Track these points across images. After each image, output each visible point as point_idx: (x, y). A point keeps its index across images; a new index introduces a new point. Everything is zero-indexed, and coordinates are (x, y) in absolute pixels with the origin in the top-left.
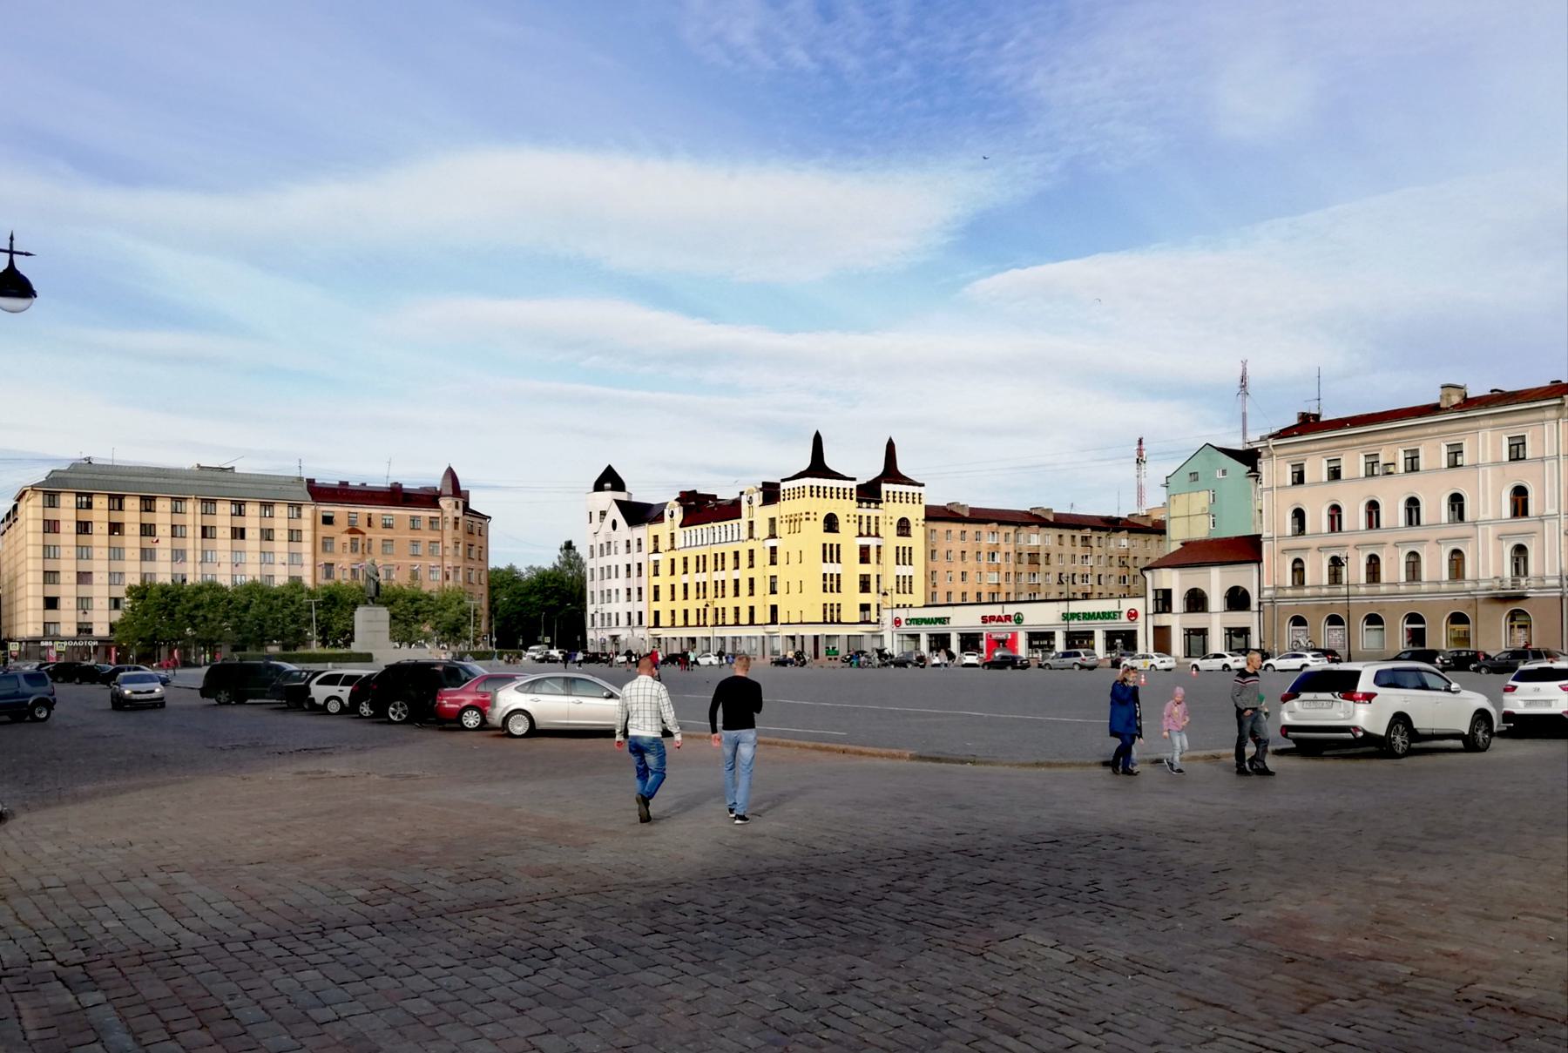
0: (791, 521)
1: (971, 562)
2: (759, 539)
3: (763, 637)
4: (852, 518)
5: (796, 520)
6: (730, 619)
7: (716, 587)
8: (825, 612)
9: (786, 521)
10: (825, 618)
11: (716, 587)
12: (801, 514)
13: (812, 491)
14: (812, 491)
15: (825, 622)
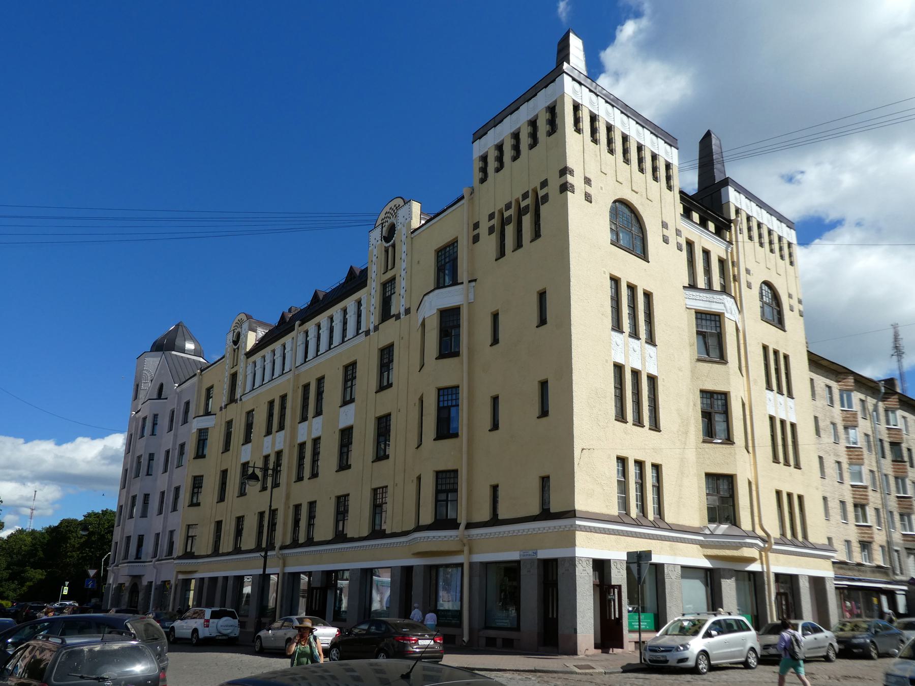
0: (504, 222)
1: (827, 438)
2: (408, 311)
3: (407, 571)
4: (671, 233)
5: (521, 212)
6: (324, 528)
7: (301, 457)
8: (623, 486)
9: (491, 230)
10: (624, 503)
11: (301, 457)
12: (544, 184)
13: (577, 121)
14: (577, 121)
15: (624, 518)
